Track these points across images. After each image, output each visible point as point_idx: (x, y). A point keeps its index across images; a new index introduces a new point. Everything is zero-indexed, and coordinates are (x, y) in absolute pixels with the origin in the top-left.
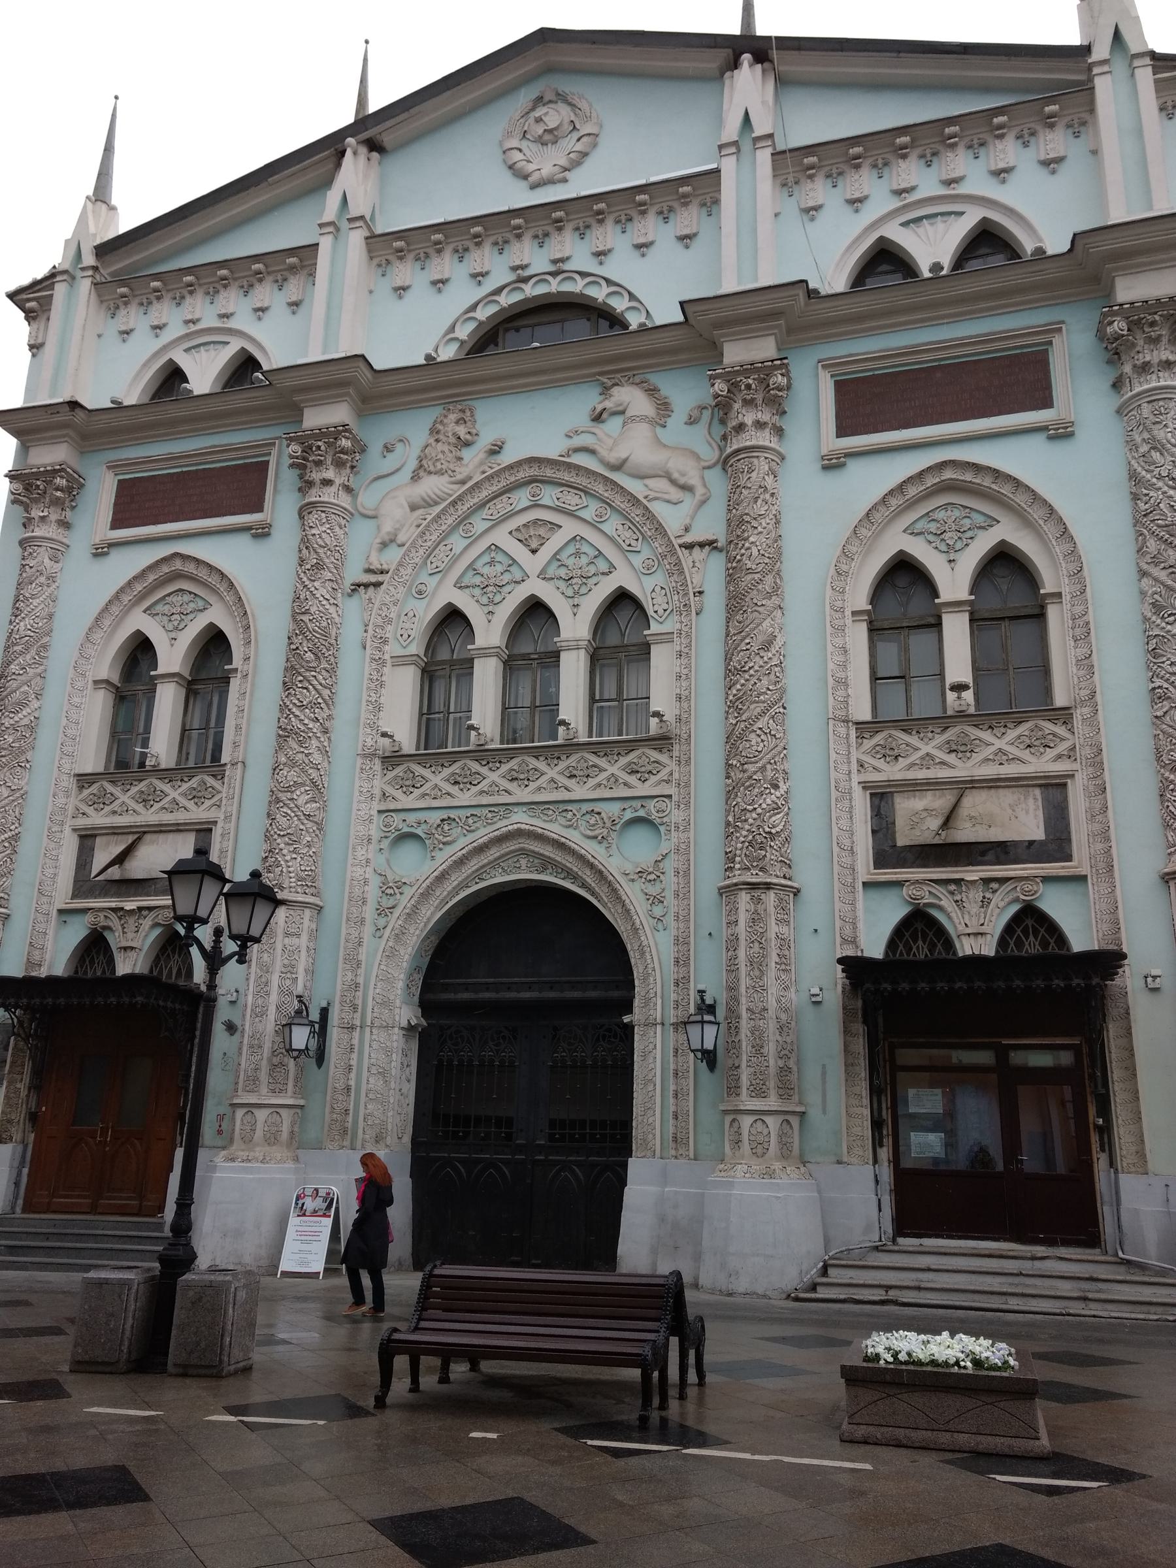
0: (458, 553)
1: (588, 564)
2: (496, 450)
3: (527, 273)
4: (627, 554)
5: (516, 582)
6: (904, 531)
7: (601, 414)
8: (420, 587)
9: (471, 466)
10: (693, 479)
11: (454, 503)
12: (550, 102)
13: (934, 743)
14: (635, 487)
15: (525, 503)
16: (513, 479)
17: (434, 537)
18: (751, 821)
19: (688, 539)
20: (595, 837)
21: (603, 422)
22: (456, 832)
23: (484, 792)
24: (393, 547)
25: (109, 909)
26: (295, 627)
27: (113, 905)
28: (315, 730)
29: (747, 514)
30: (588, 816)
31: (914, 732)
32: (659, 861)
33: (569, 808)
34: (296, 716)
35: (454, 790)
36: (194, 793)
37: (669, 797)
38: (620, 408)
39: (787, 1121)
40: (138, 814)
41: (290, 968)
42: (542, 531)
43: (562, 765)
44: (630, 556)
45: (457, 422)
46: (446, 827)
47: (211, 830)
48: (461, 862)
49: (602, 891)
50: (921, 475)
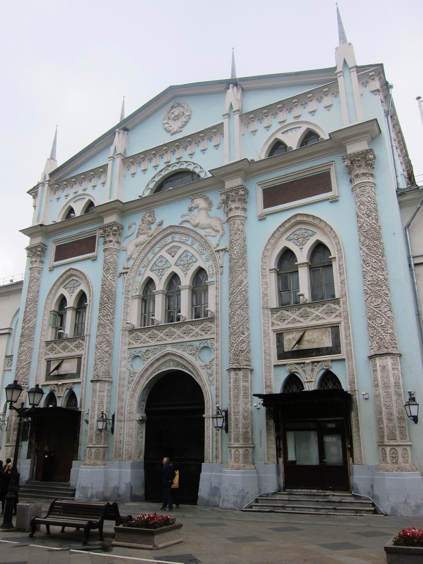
0: (150, 259)
2: (161, 224)
6: (286, 239)
10: (219, 228)
11: (148, 243)
12: (176, 107)
13: (296, 314)
14: (202, 232)
15: (170, 241)
16: (166, 233)
17: (143, 255)
18: (235, 346)
19: (218, 249)
20: (191, 354)
23: (159, 340)
24: (131, 259)
27: (55, 383)
28: (108, 323)
29: (233, 239)
30: (189, 347)
31: (290, 311)
33: (184, 344)
34: (102, 319)
35: (150, 340)
36: (77, 346)
37: (214, 338)
38: (197, 206)
39: (247, 450)
41: (101, 402)
42: (175, 250)
44: (202, 255)
46: (147, 353)
48: (152, 364)
50: (289, 219)
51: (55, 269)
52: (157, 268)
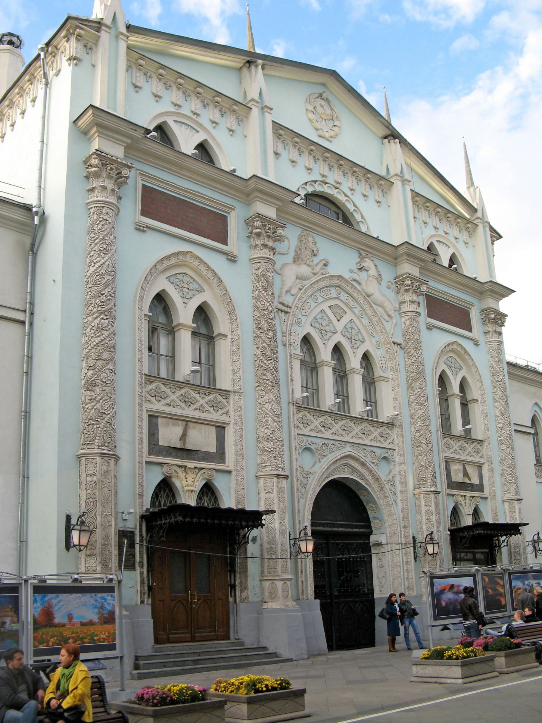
3: (327, 181)
7: (361, 269)
15: (335, 296)
20: (374, 463)
25: (177, 465)
27: (180, 463)
30: (371, 453)
36: (213, 404)
37: (394, 450)
38: (368, 269)
40: (183, 409)
51: (149, 232)
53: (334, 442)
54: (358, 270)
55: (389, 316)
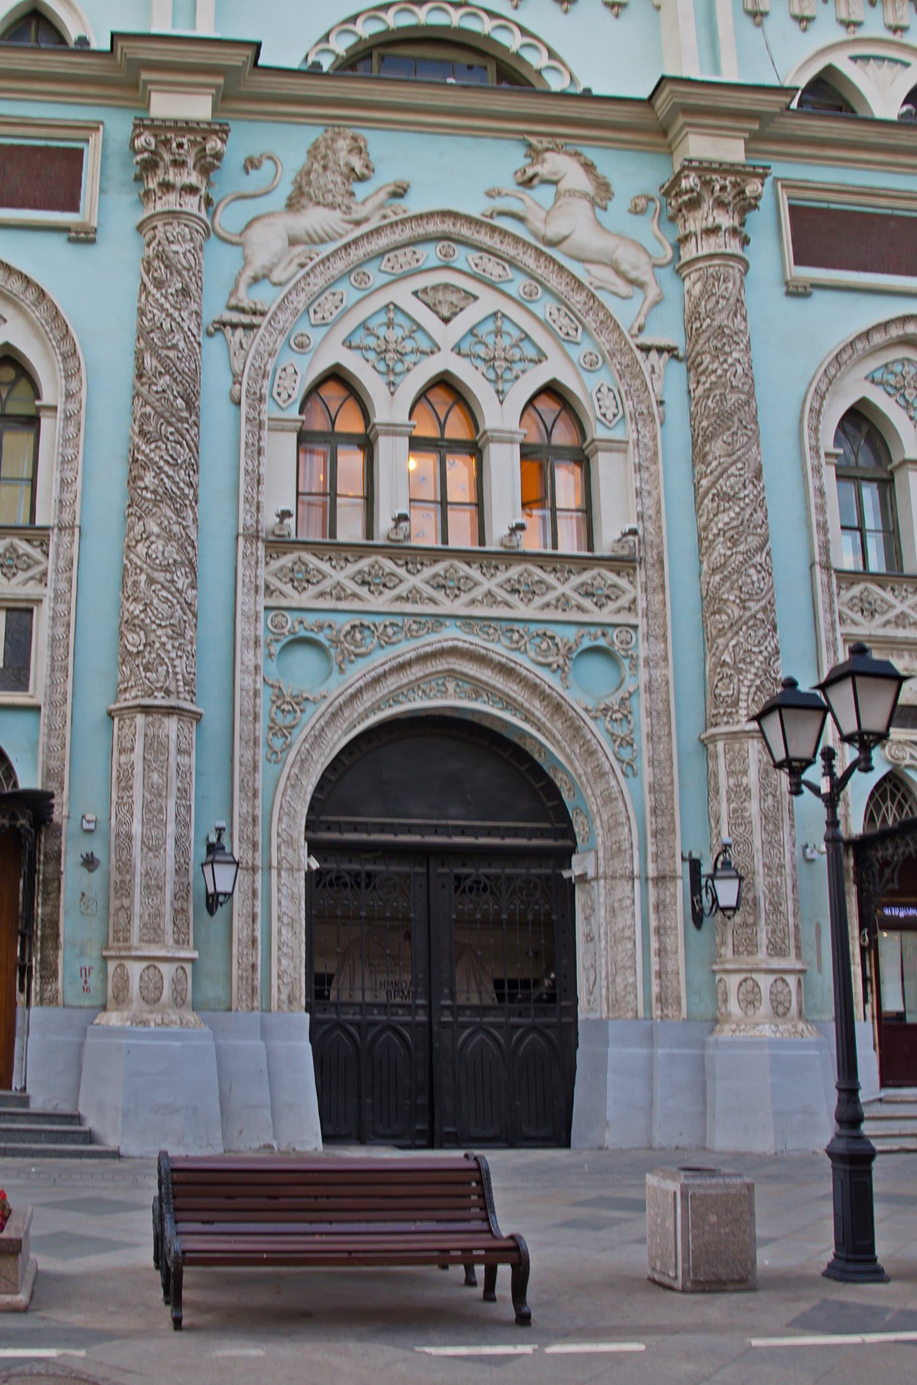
0: (350, 305)
1: (512, 346)
2: (399, 192)
4: (565, 345)
5: (423, 353)
7: (531, 179)
8: (300, 339)
9: (370, 205)
11: (347, 246)
15: (436, 263)
16: (421, 231)
19: (646, 339)
20: (549, 665)
21: (531, 188)
22: (371, 642)
26: (155, 363)
30: (538, 640)
32: (626, 699)
34: (168, 477)
35: (363, 591)
37: (635, 627)
38: (555, 178)
42: (454, 298)
43: (501, 576)
44: (569, 348)
45: (350, 151)
46: (358, 636)
47: (30, 611)
49: (557, 727)
52: (371, 342)
53: (398, 620)
54: (521, 188)
55: (633, 282)
